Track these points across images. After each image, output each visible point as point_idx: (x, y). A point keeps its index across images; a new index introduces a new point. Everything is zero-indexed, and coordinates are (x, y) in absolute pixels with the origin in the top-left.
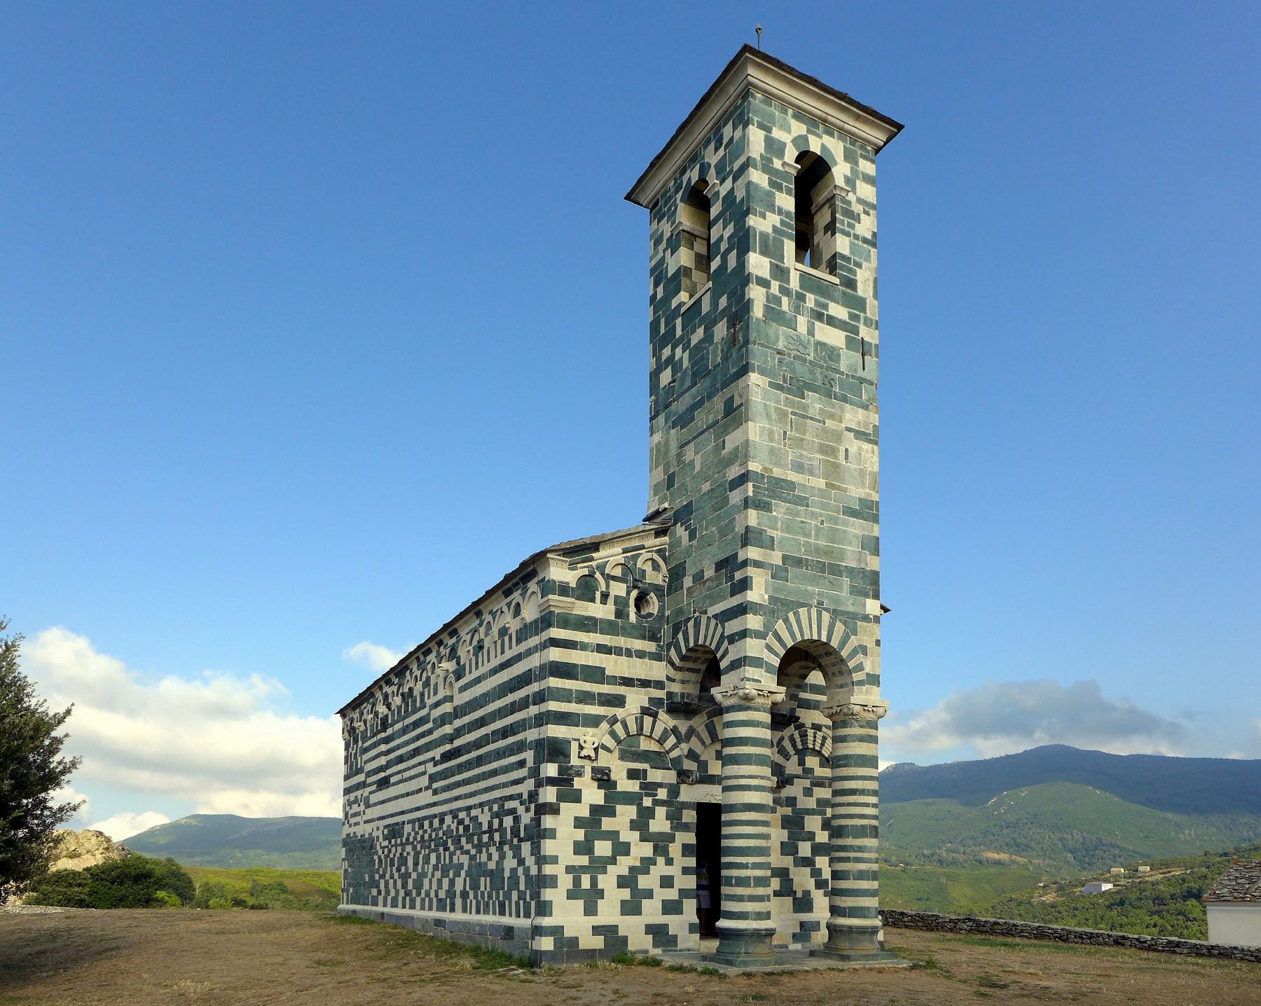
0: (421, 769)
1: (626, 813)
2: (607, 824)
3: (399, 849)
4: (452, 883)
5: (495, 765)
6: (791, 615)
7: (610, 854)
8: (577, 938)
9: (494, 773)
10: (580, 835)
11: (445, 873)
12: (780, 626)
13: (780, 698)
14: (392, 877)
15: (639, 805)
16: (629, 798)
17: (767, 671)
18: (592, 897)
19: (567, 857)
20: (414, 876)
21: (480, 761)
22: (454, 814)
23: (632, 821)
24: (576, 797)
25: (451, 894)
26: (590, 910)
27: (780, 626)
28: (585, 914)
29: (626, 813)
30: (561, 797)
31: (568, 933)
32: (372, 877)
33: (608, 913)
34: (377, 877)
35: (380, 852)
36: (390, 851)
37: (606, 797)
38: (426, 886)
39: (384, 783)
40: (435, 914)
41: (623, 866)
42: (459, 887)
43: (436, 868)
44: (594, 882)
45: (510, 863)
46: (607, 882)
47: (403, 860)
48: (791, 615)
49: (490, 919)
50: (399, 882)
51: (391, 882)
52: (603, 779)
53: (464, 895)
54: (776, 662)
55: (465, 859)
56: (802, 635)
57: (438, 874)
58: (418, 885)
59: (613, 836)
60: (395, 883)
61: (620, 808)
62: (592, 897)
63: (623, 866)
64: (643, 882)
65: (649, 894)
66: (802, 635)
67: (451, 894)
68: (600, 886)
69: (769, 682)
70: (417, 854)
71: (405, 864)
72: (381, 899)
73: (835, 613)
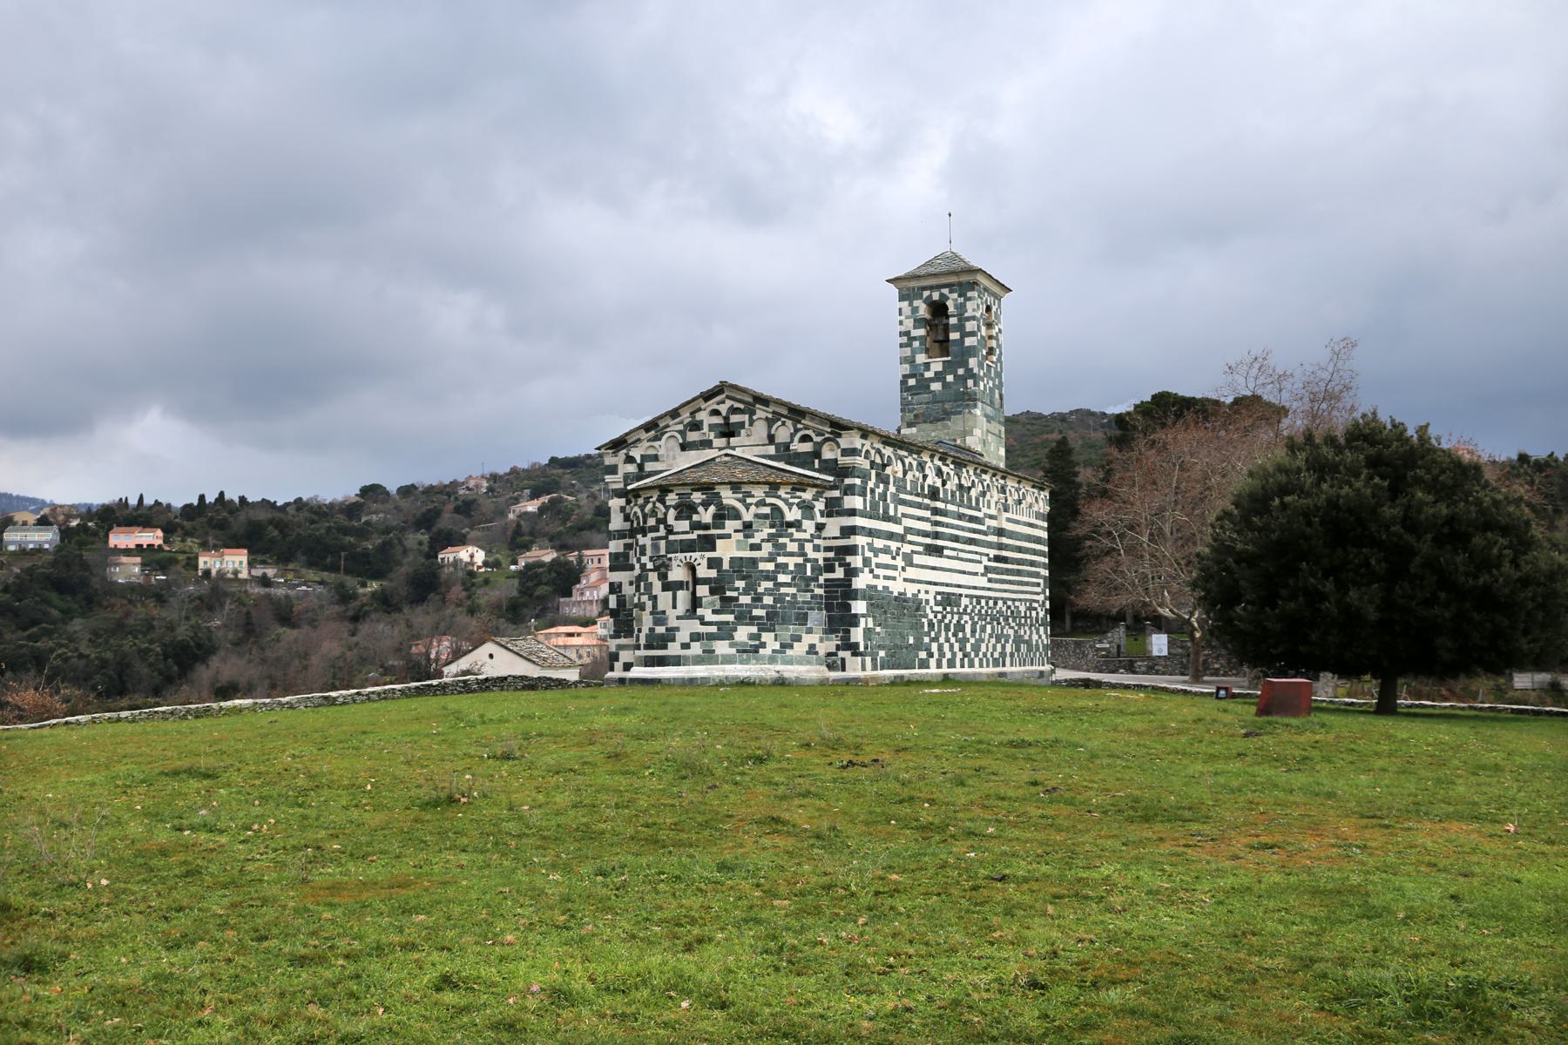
0: (977, 557)
3: (956, 617)
4: (1004, 647)
5: (1026, 579)
9: (1027, 584)
11: (998, 641)
14: (947, 640)
20: (972, 641)
21: (1019, 573)
22: (1005, 601)
25: (1003, 654)
32: (919, 639)
34: (926, 640)
35: (931, 616)
36: (944, 617)
38: (983, 649)
39: (936, 551)
40: (992, 670)
42: (1008, 650)
43: (991, 636)
45: (1035, 637)
47: (960, 627)
49: (1028, 668)
50: (956, 646)
51: (946, 646)
53: (1012, 655)
55: (1011, 632)
57: (993, 641)
58: (976, 648)
60: (952, 646)
67: (1003, 654)
70: (974, 624)
71: (963, 630)
72: (933, 662)
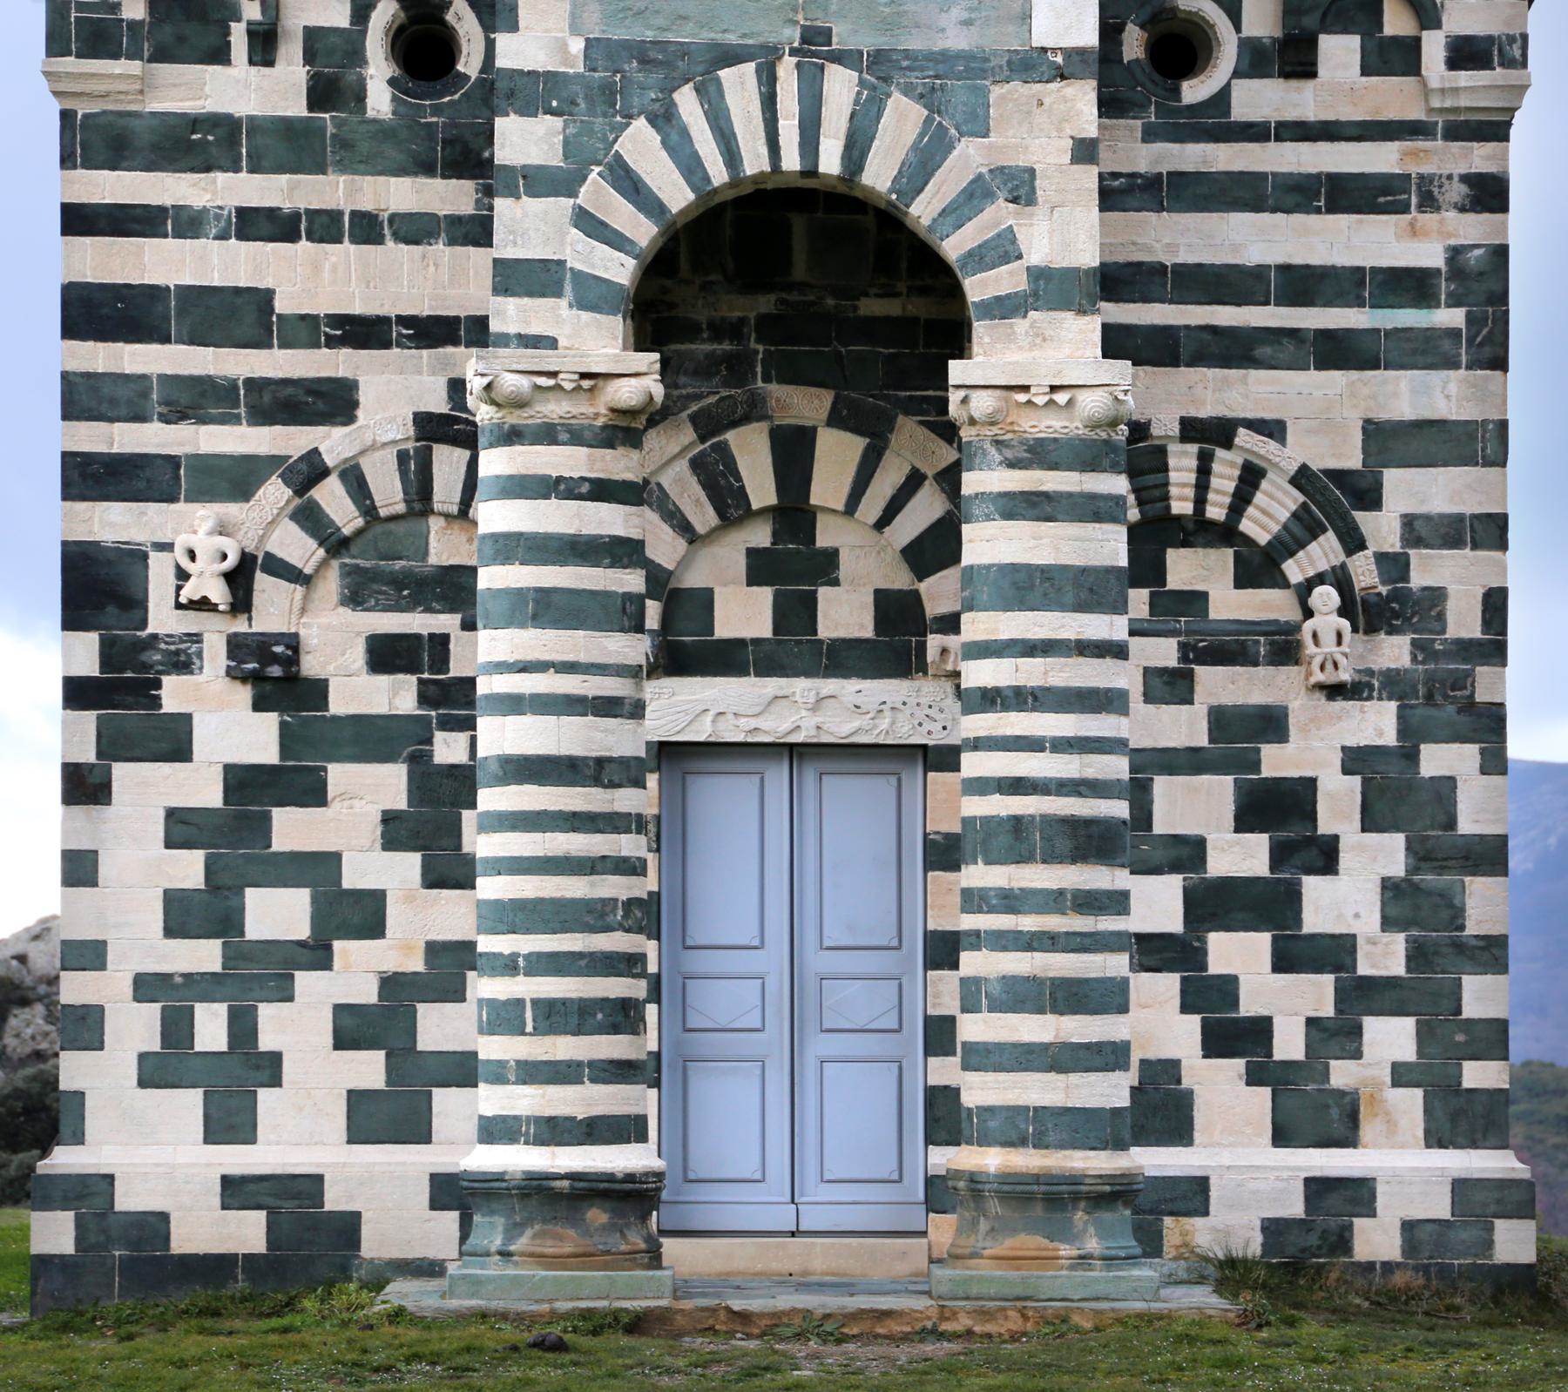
1: (369, 790)
2: (291, 829)
6: (687, 102)
7: (303, 932)
8: (164, 1217)
10: (189, 869)
12: (640, 144)
13: (626, 393)
15: (420, 762)
16: (372, 739)
17: (581, 304)
18: (234, 1089)
19: (141, 942)
23: (389, 818)
24: (173, 742)
26: (229, 1122)
27: (640, 144)
28: (211, 1137)
29: (369, 790)
30: (114, 746)
31: (128, 1200)
33: (300, 1129)
37: (287, 738)
41: (357, 972)
44: (242, 1028)
46: (295, 1026)
48: (687, 102)
52: (275, 675)
54: (620, 270)
56: (732, 157)
59: (317, 869)
61: (339, 775)
62: (234, 1089)
63: (357, 972)
64: (440, 1028)
65: (463, 1070)
66: (732, 157)
68: (266, 1043)
69: (598, 341)
73: (880, 69)
